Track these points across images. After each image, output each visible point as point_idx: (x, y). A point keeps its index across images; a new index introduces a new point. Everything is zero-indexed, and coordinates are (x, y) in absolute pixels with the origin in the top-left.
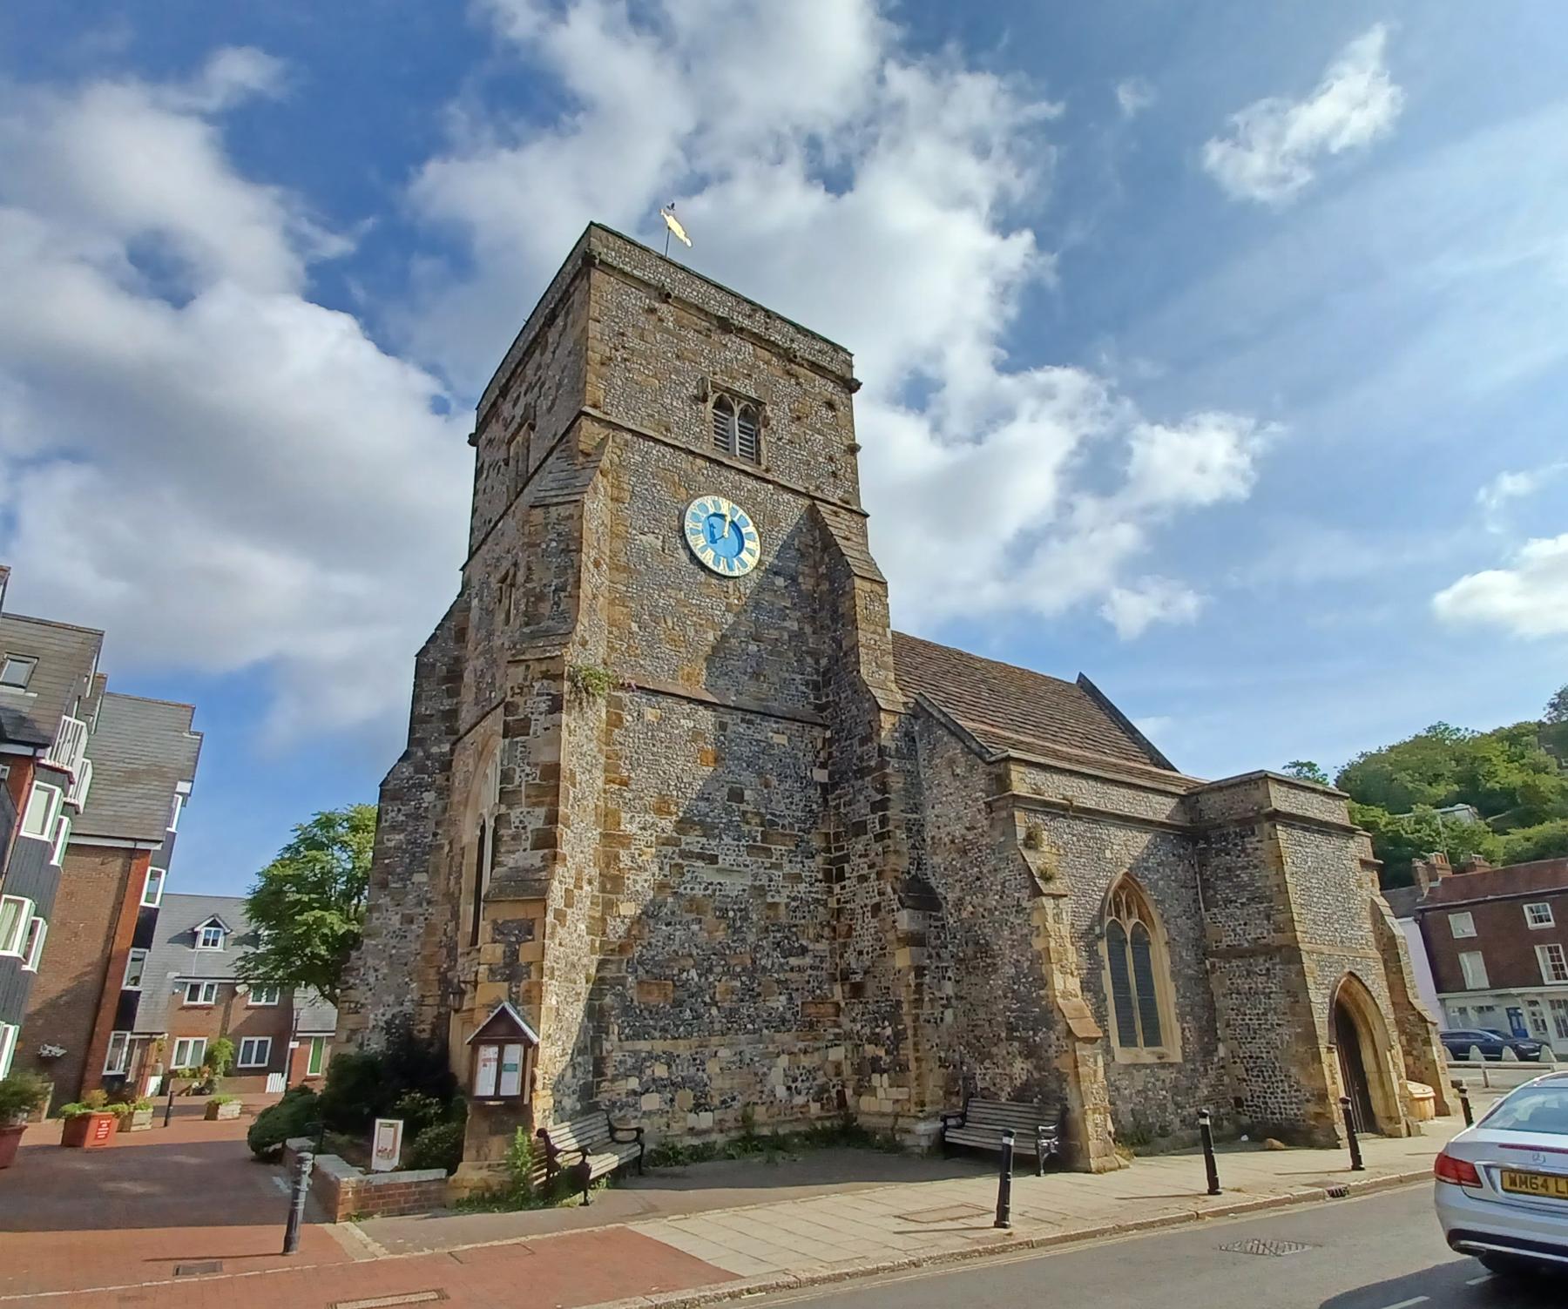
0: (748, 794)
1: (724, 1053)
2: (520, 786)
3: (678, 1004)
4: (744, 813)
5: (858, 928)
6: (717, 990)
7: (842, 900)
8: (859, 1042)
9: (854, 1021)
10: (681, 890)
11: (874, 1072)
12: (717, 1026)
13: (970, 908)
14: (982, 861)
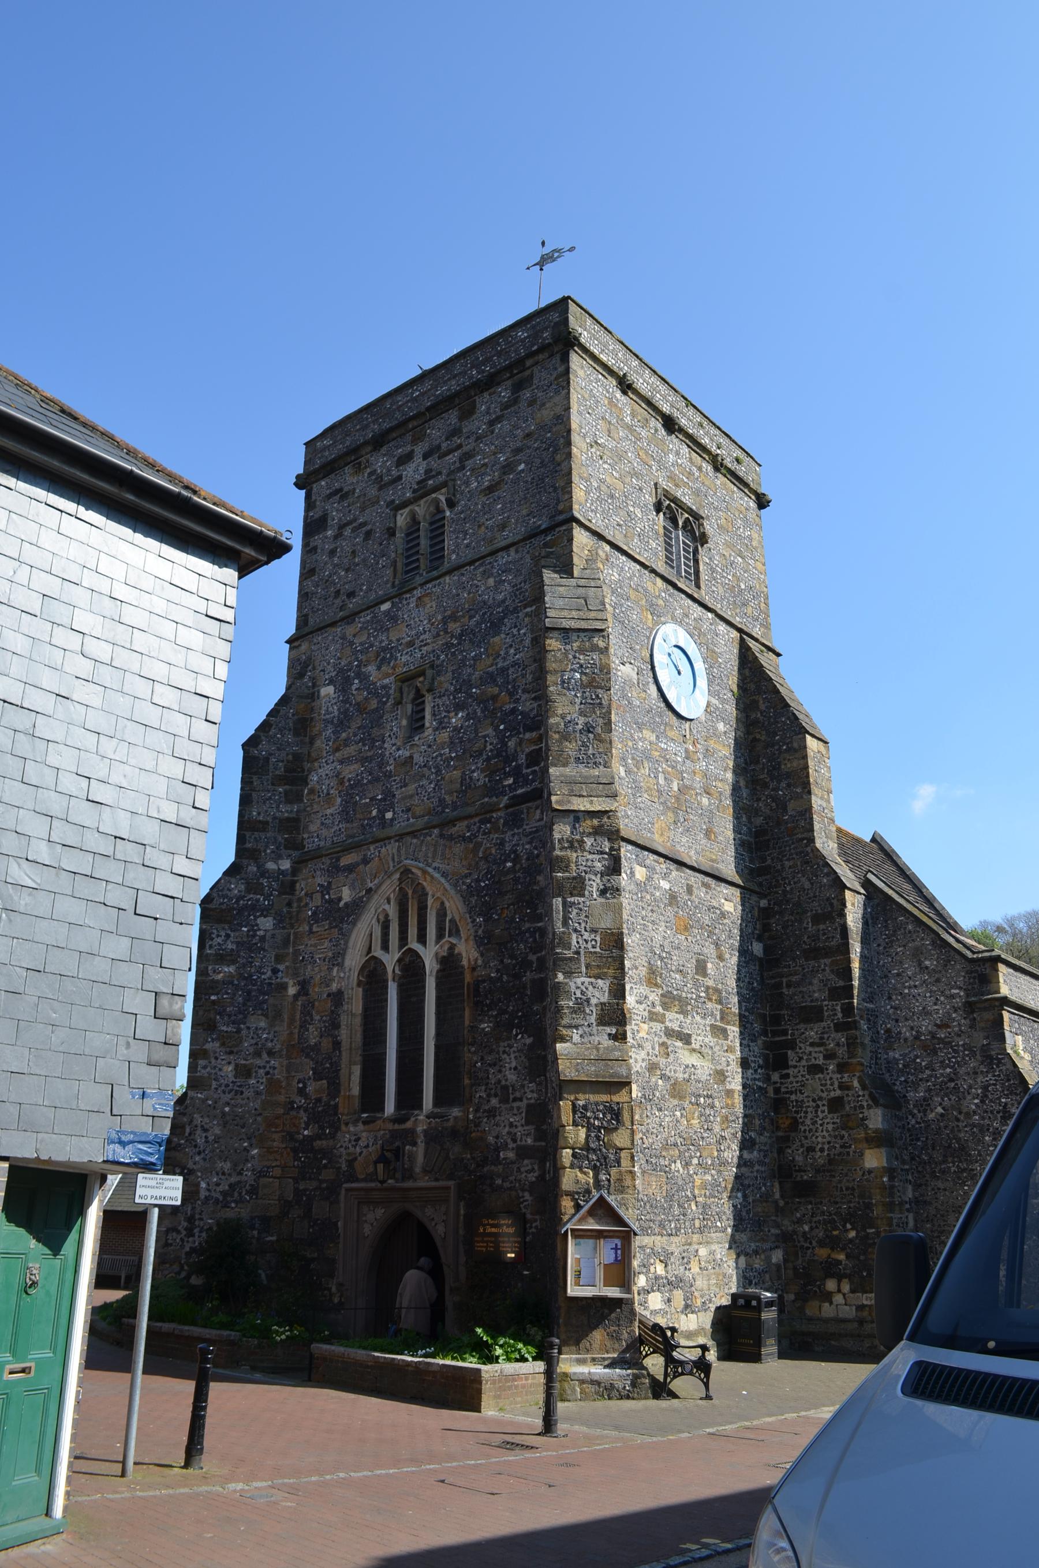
0: (709, 965)
1: (703, 1252)
2: (578, 953)
3: (669, 1197)
4: (708, 988)
5: (808, 1122)
6: (696, 1184)
7: (783, 1090)
8: (807, 1245)
9: (799, 1222)
10: (668, 1073)
11: (830, 1275)
12: (697, 1223)
13: (940, 1110)
14: (958, 1062)
